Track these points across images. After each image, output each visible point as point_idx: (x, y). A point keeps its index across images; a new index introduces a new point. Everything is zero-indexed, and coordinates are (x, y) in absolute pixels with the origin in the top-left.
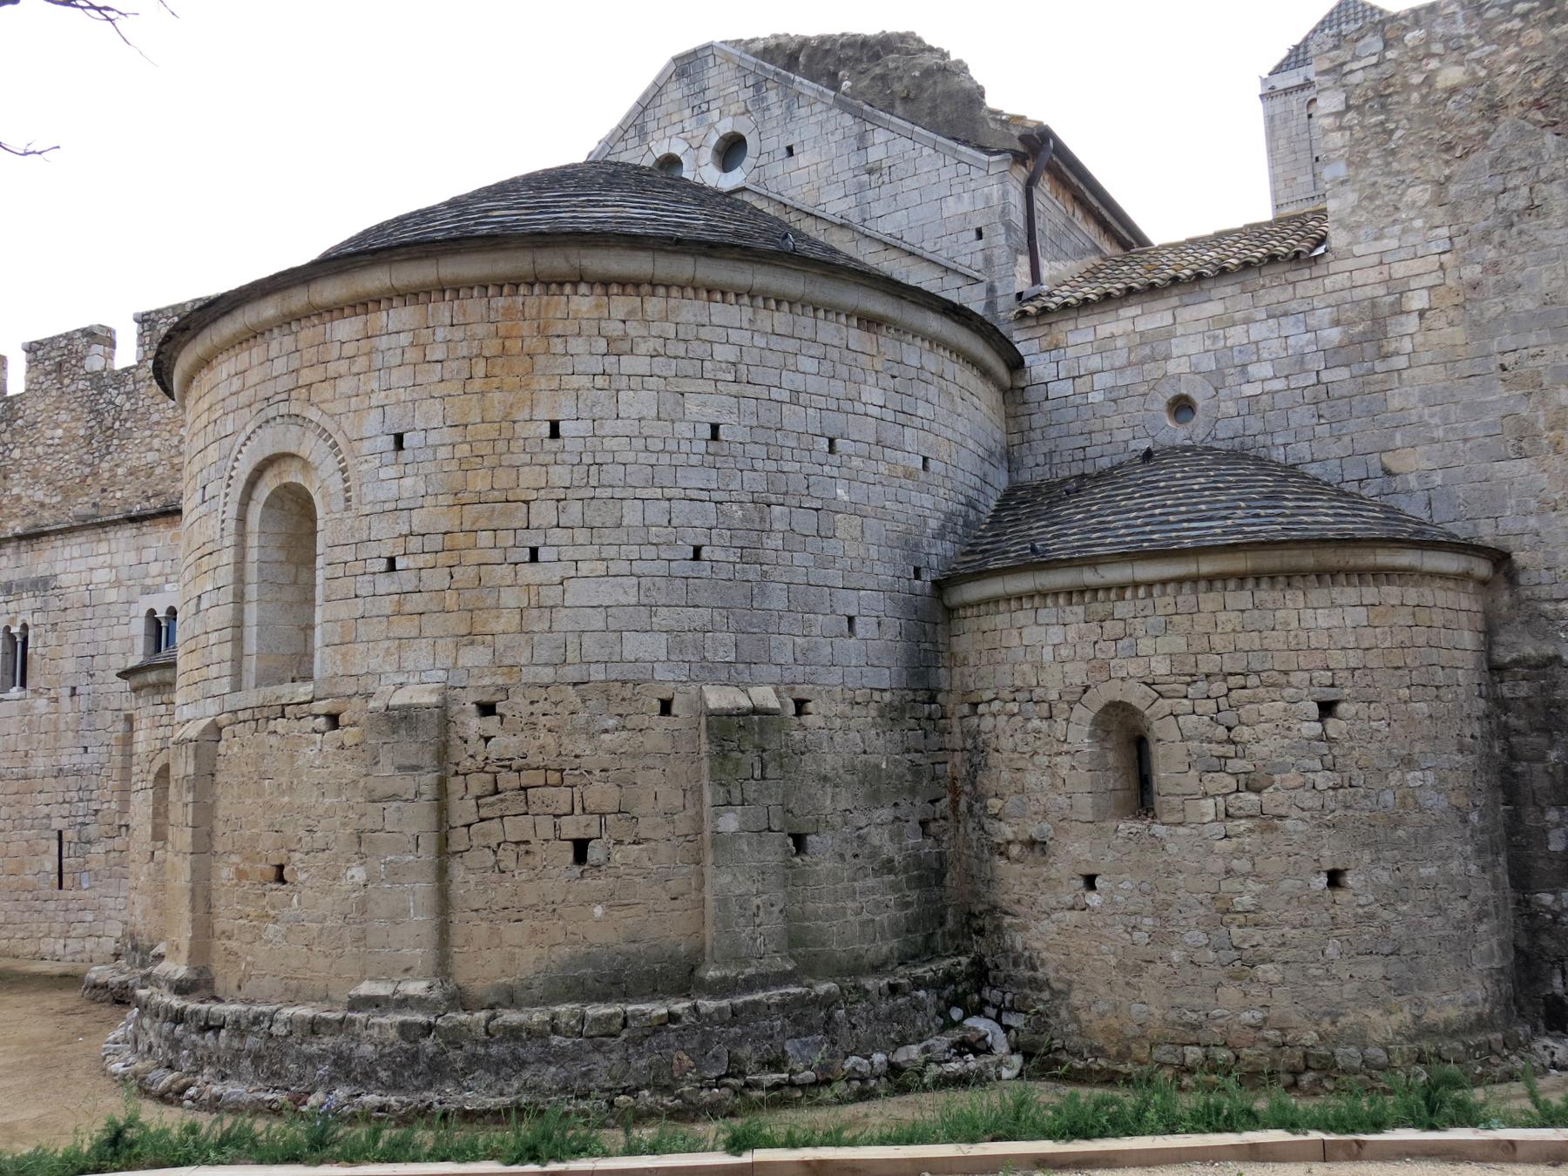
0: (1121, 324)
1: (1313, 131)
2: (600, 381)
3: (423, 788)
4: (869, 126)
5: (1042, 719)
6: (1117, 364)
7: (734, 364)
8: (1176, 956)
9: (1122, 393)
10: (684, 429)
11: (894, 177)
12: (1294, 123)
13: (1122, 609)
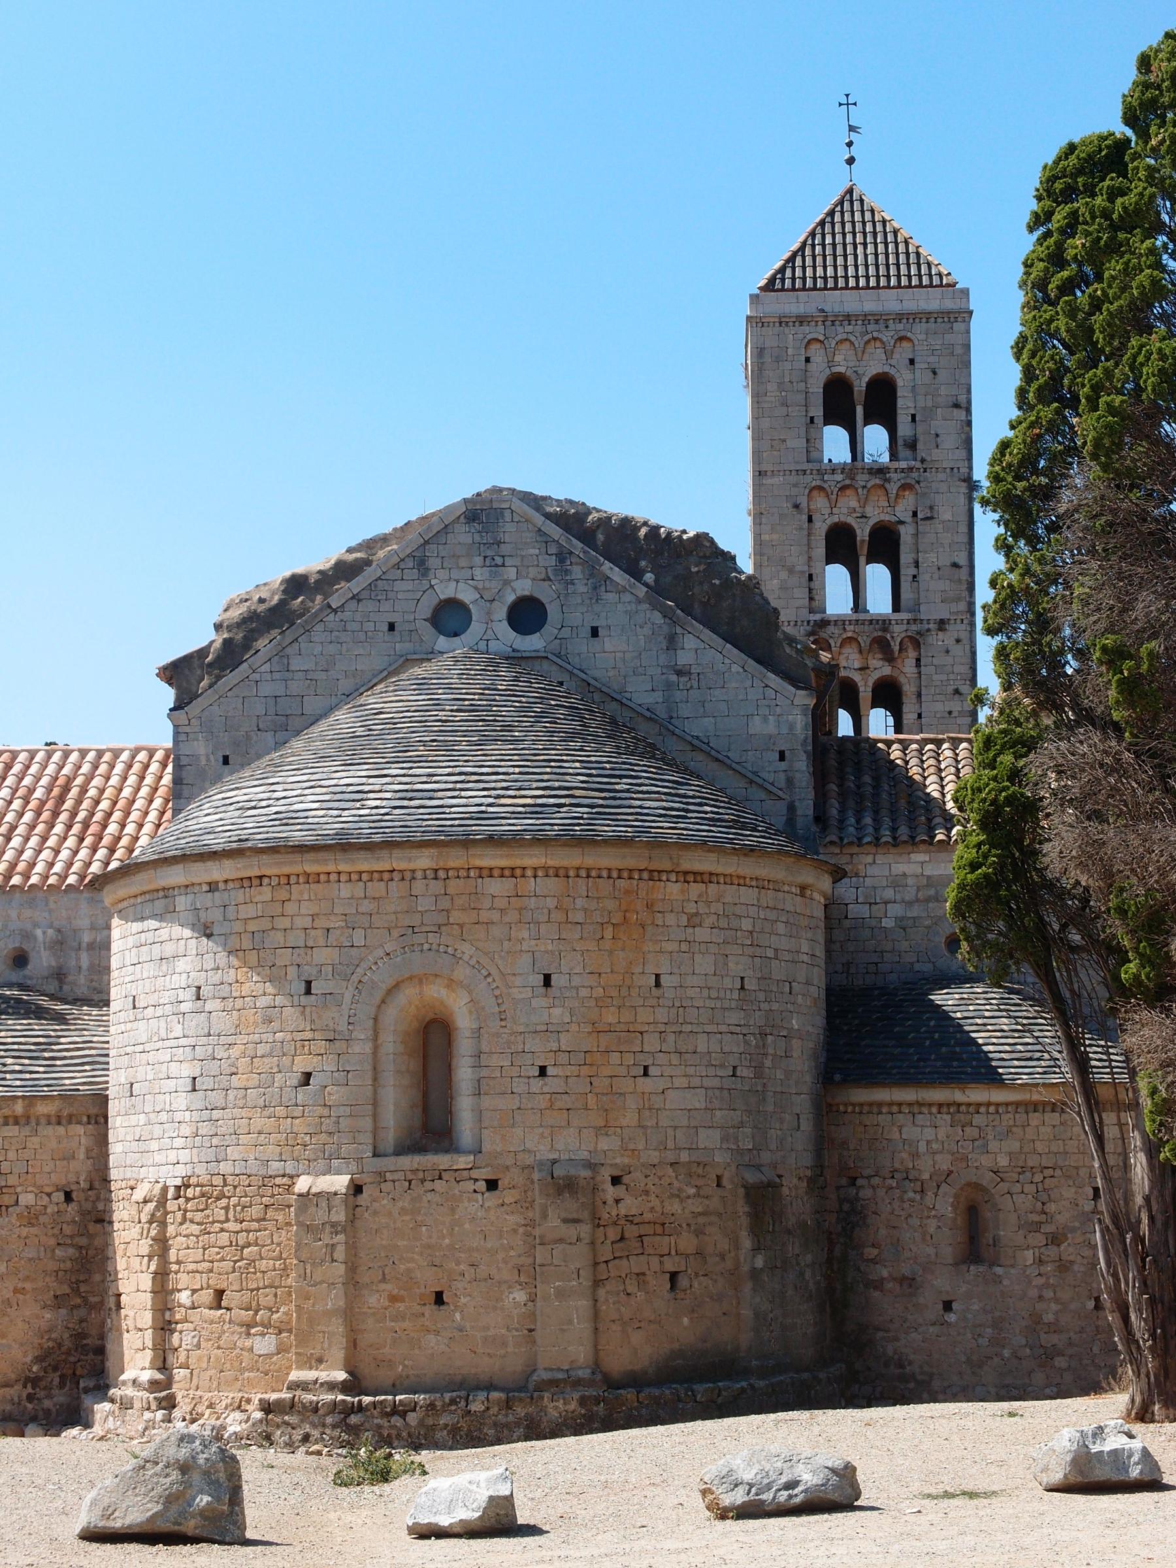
0: (912, 866)
1: (810, 381)
2: (684, 947)
3: (582, 1235)
4: (679, 630)
5: (915, 1192)
6: (907, 898)
7: (751, 932)
8: (1006, 1353)
9: (910, 923)
10: (727, 982)
11: (703, 684)
12: (788, 365)
13: (978, 1120)
